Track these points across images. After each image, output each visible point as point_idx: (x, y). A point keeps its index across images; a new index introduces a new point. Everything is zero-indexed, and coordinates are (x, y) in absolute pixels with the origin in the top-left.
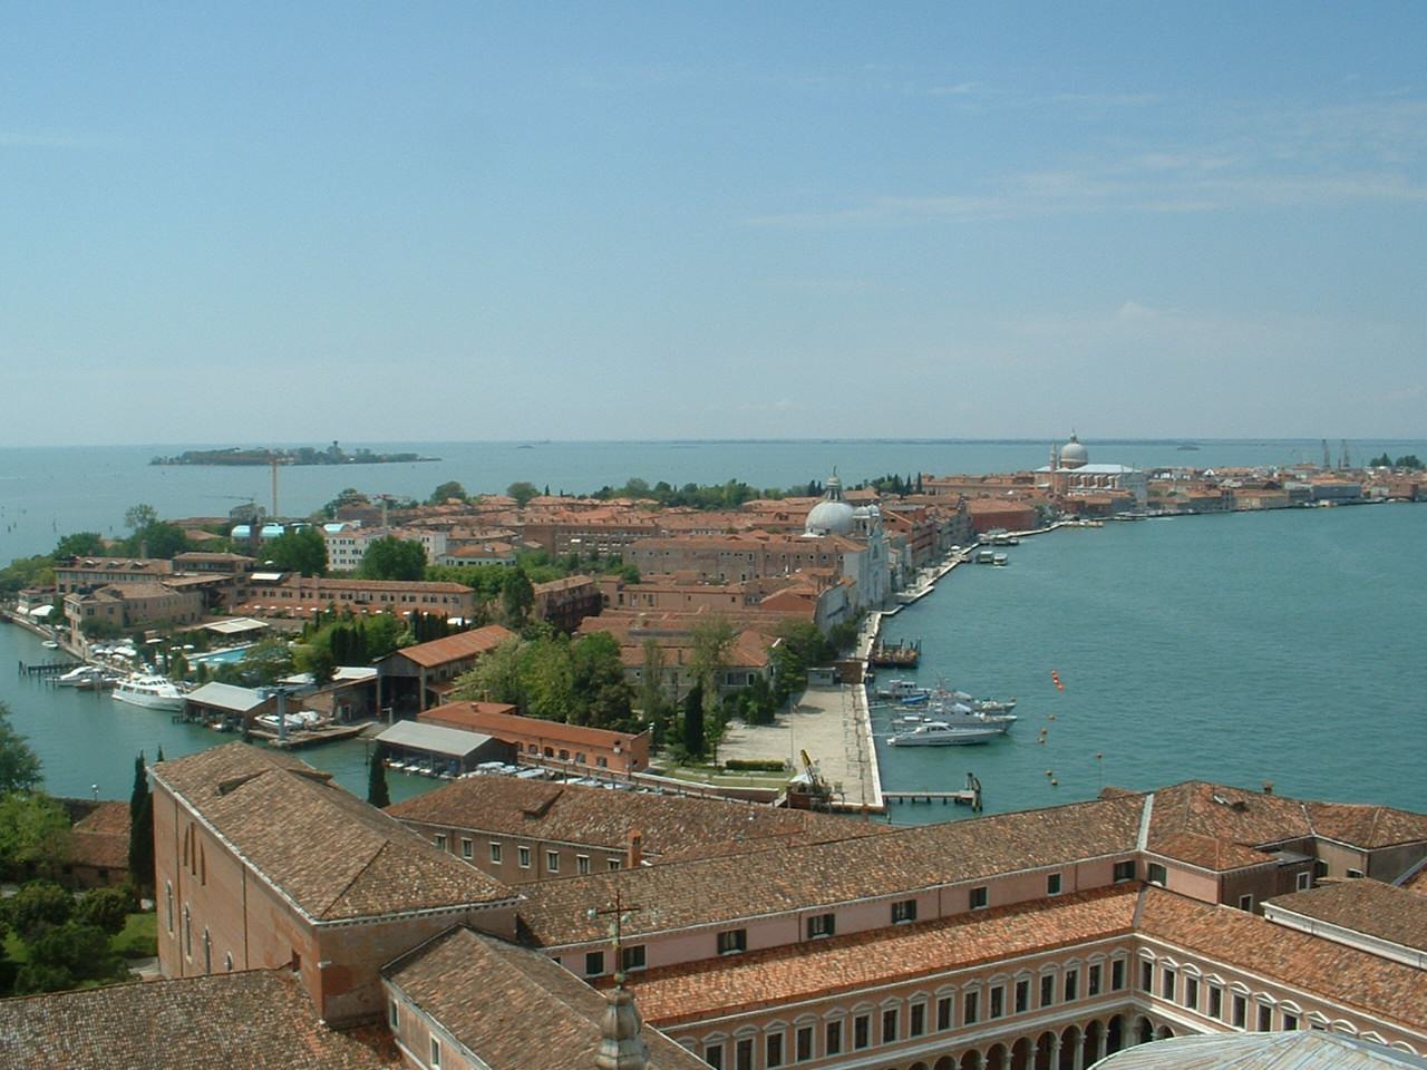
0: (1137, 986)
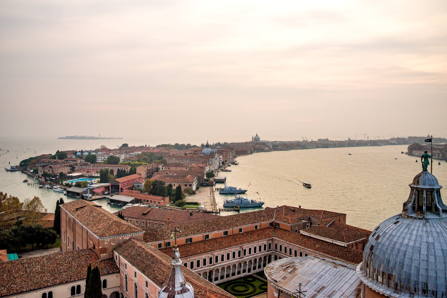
0: (274, 249)
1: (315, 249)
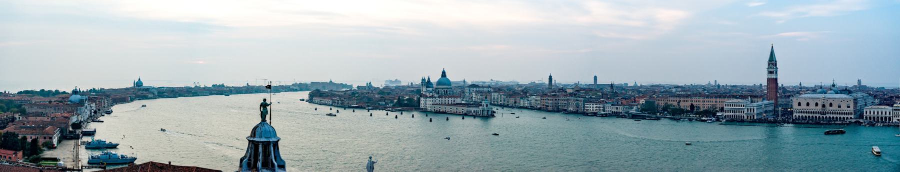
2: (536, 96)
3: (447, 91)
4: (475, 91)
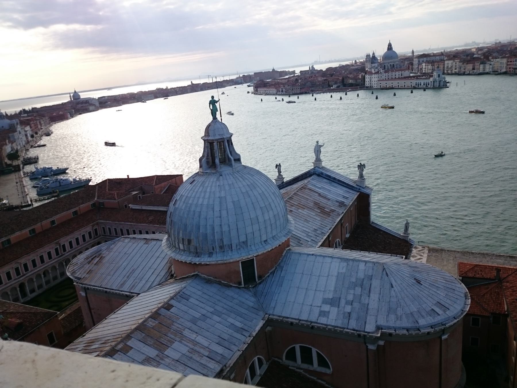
1: (148, 222)
2: (501, 58)
3: (393, 65)
4: (425, 61)
